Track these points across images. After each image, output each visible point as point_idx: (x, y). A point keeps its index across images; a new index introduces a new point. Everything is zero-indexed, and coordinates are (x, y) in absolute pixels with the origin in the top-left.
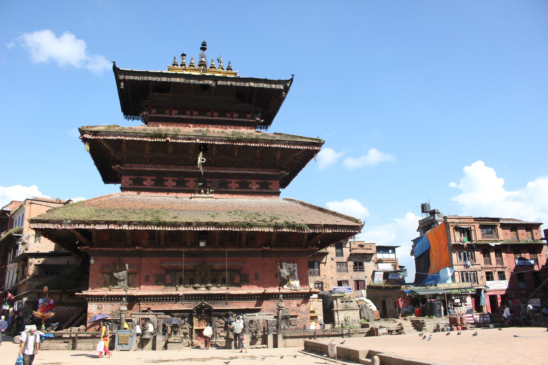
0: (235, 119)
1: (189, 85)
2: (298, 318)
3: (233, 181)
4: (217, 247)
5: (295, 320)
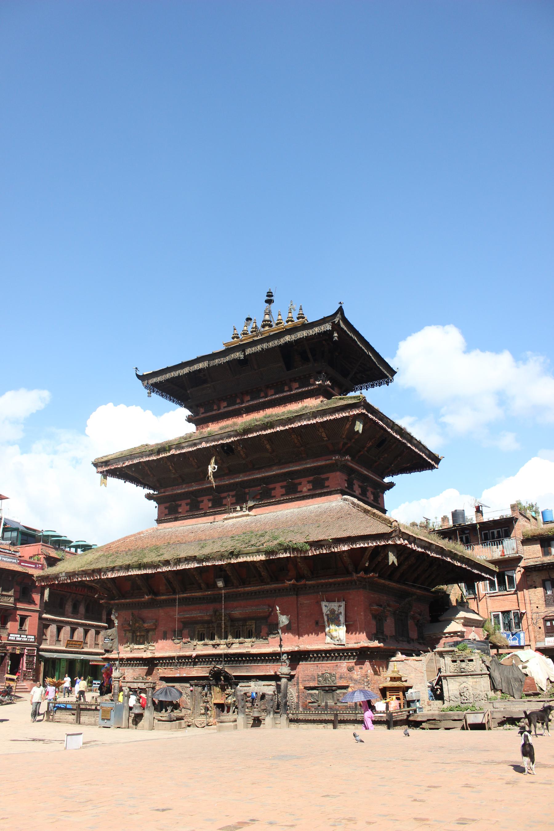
2: (350, 690)
3: (278, 485)
4: (237, 587)
5: (344, 694)
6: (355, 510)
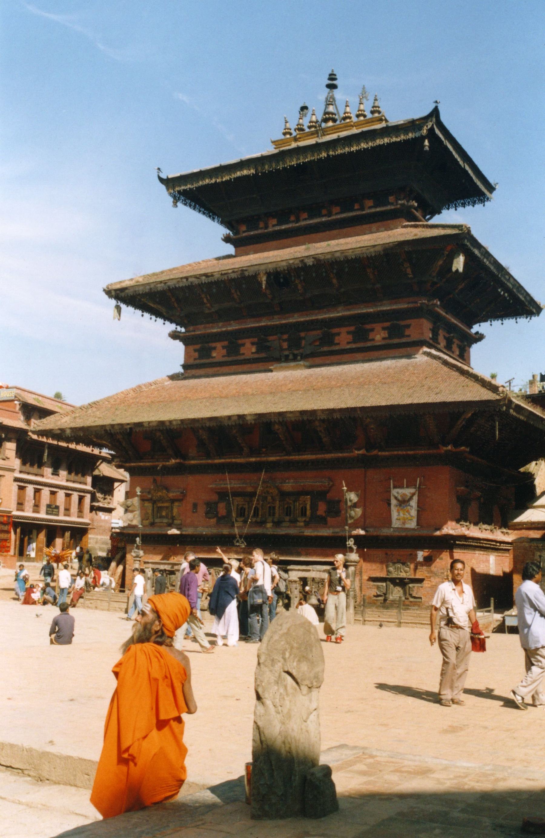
0: (369, 211)
3: (344, 330)
4: (290, 455)
6: (446, 369)
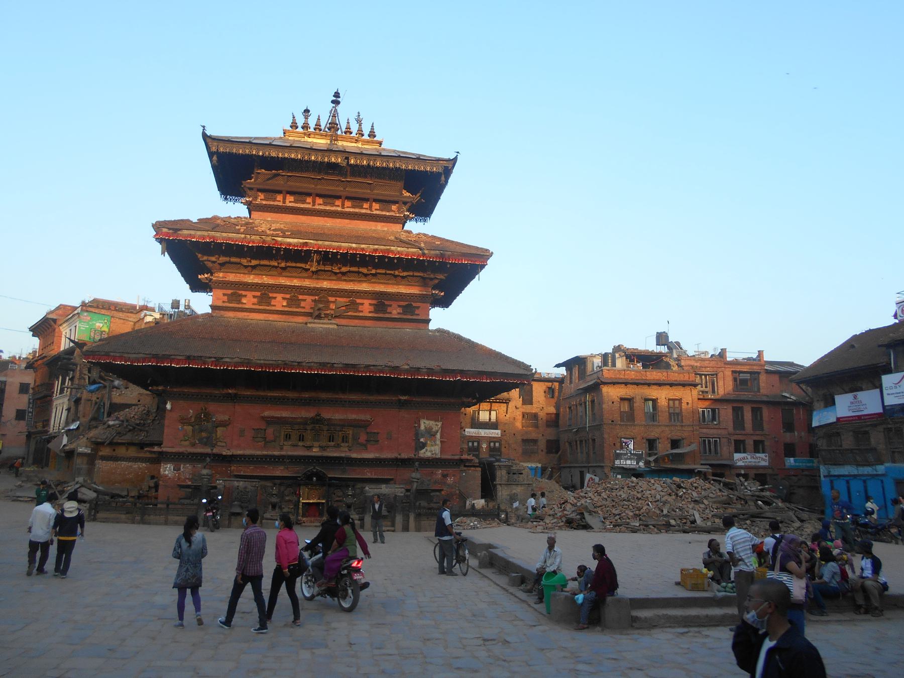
1: (309, 162)
